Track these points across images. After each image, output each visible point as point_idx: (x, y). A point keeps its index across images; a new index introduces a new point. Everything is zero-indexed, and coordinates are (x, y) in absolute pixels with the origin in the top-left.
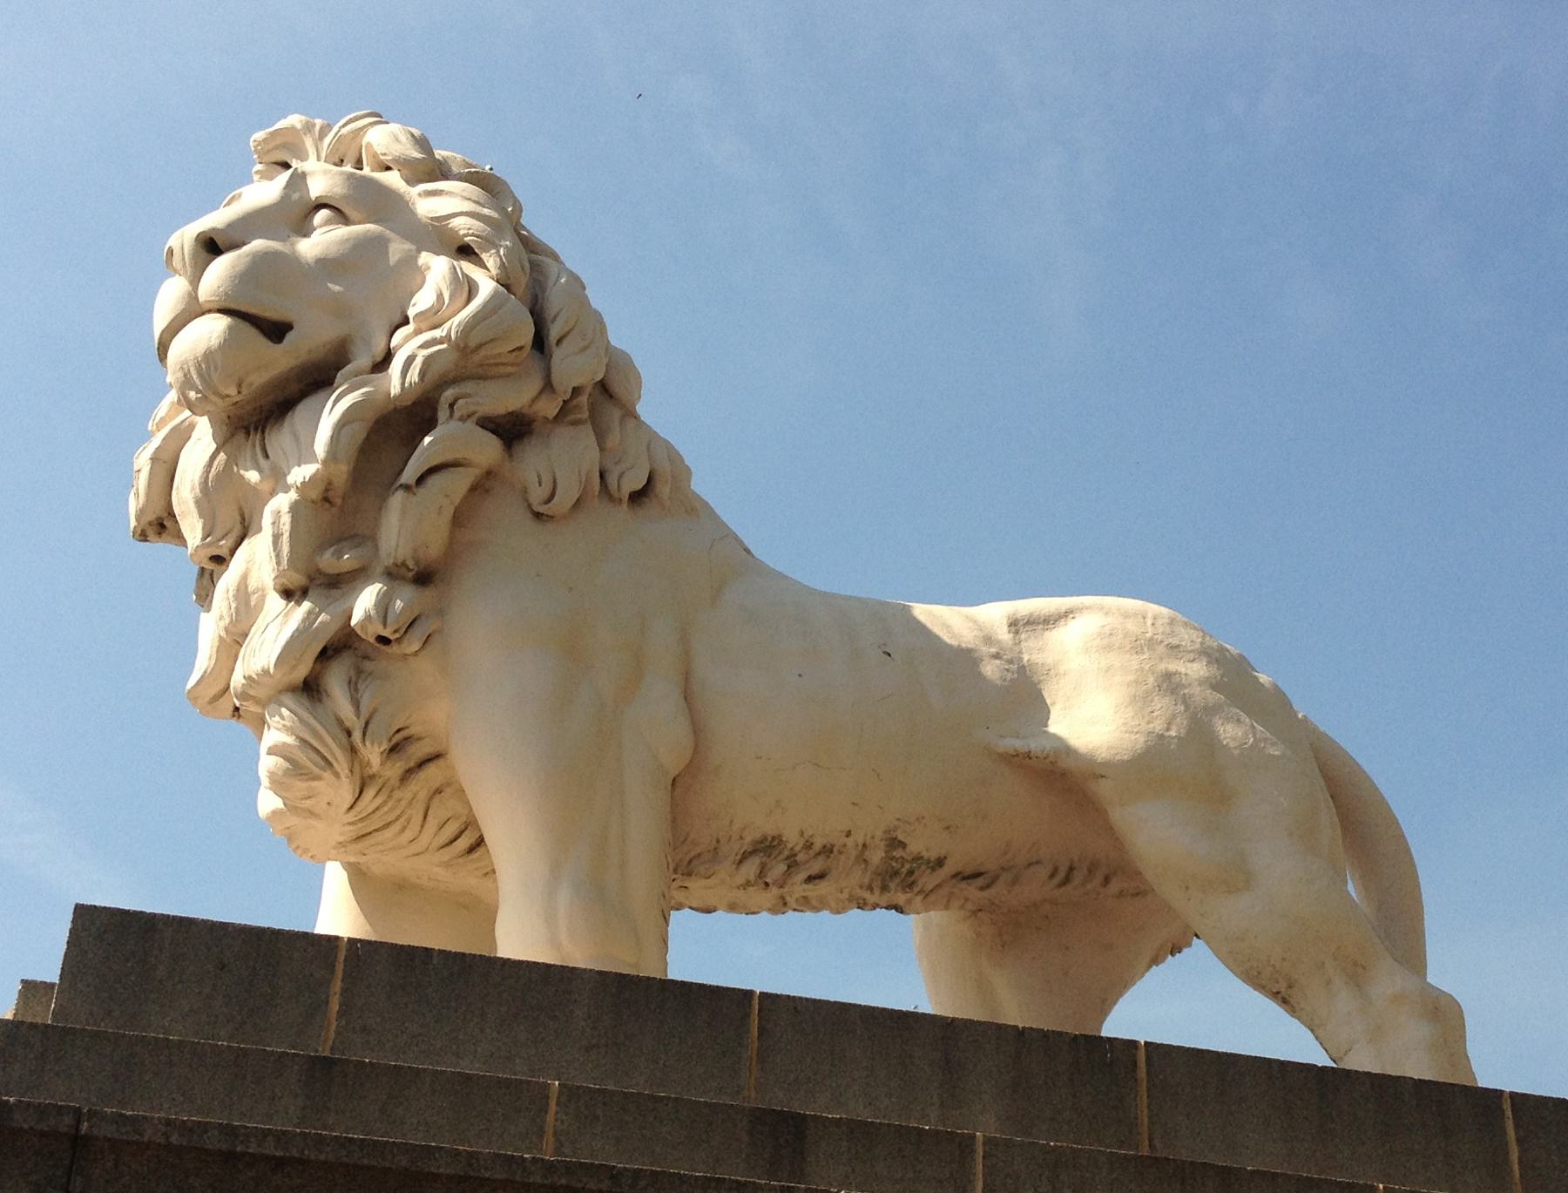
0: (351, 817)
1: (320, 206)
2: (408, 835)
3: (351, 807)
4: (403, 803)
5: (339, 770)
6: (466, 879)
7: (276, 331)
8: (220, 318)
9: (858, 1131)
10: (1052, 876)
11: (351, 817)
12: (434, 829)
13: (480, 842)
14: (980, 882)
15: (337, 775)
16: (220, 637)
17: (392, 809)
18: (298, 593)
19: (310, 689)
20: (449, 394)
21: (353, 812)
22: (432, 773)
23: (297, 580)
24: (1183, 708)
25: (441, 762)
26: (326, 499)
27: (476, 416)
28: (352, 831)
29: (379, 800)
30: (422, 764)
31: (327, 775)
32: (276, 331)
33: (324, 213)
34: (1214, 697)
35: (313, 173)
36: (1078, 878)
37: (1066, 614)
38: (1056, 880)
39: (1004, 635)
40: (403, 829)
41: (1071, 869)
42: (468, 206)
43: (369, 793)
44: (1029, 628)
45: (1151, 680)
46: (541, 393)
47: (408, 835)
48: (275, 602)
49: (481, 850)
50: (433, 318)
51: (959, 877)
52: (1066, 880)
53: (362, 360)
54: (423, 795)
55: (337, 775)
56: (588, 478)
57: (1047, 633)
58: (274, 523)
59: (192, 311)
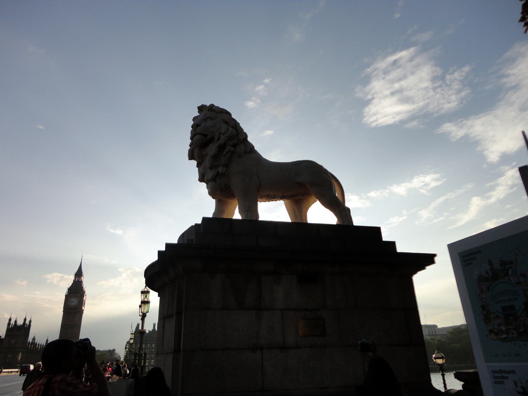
7: (206, 136)
20: (228, 143)
33: (209, 119)
52: (303, 196)
53: (216, 138)
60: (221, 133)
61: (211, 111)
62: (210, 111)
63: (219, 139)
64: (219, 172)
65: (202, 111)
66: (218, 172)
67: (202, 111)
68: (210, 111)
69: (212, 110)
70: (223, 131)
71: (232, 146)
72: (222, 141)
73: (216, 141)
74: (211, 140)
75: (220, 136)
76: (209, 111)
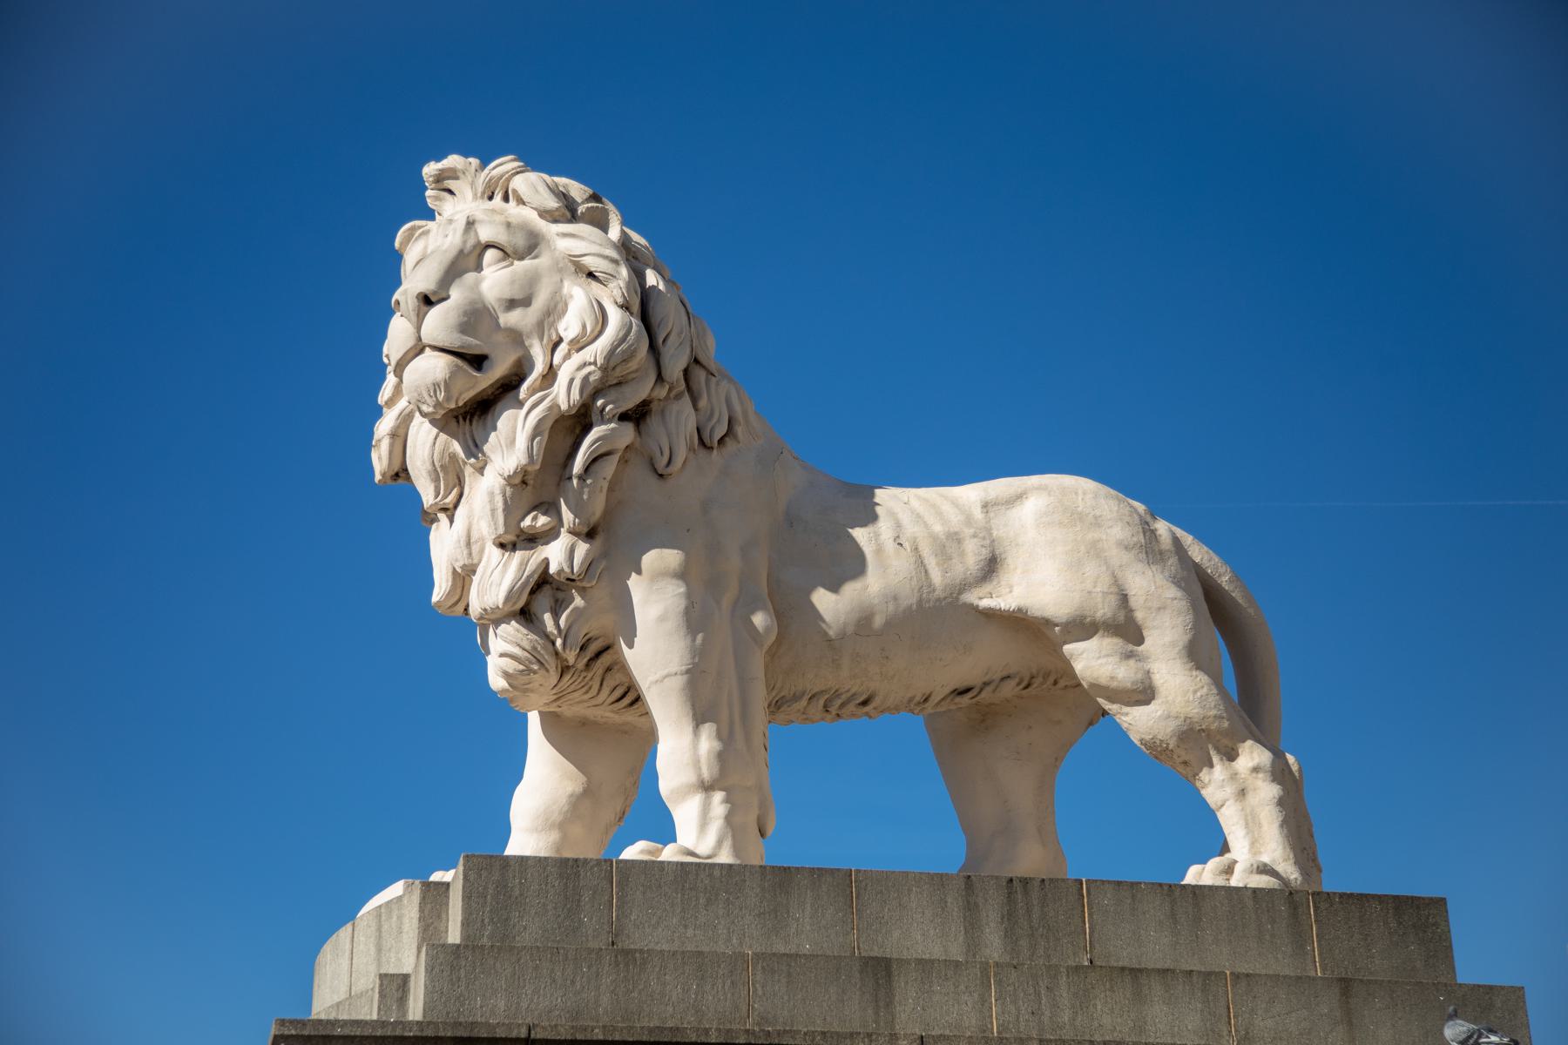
0: (554, 691)
1: (488, 246)
2: (589, 695)
3: (555, 686)
4: (587, 679)
5: (548, 667)
6: (630, 717)
7: (477, 361)
8: (439, 356)
9: (925, 965)
10: (1018, 684)
11: (554, 691)
12: (608, 692)
13: (638, 699)
14: (970, 694)
15: (547, 671)
16: (454, 569)
17: (583, 681)
18: (510, 546)
19: (525, 615)
20: (600, 403)
21: (556, 689)
22: (605, 660)
23: (510, 538)
24: (1105, 568)
25: (610, 651)
26: (524, 482)
27: (618, 415)
28: (555, 697)
29: (574, 678)
30: (598, 655)
31: (543, 672)
32: (477, 361)
34: (1127, 557)
35: (481, 222)
36: (1037, 682)
37: (1019, 497)
38: (1021, 687)
39: (978, 514)
40: (587, 692)
41: (1032, 677)
42: (595, 249)
43: (567, 677)
44: (995, 508)
45: (1083, 548)
46: (656, 381)
47: (589, 695)
48: (493, 553)
49: (640, 703)
50: (579, 345)
51: (956, 692)
52: (1026, 687)
54: (600, 672)
55: (547, 671)
56: (691, 437)
57: (1008, 512)
58: (490, 501)
59: (419, 349)
60: (560, 340)
61: (506, 199)
62: (498, 198)
63: (550, 375)
64: (553, 569)
65: (450, 192)
66: (546, 562)
67: (450, 192)
68: (498, 198)
69: (510, 192)
70: (569, 327)
71: (623, 417)
72: (564, 394)
73: (533, 392)
74: (508, 387)
75: (557, 359)
76: (491, 198)
